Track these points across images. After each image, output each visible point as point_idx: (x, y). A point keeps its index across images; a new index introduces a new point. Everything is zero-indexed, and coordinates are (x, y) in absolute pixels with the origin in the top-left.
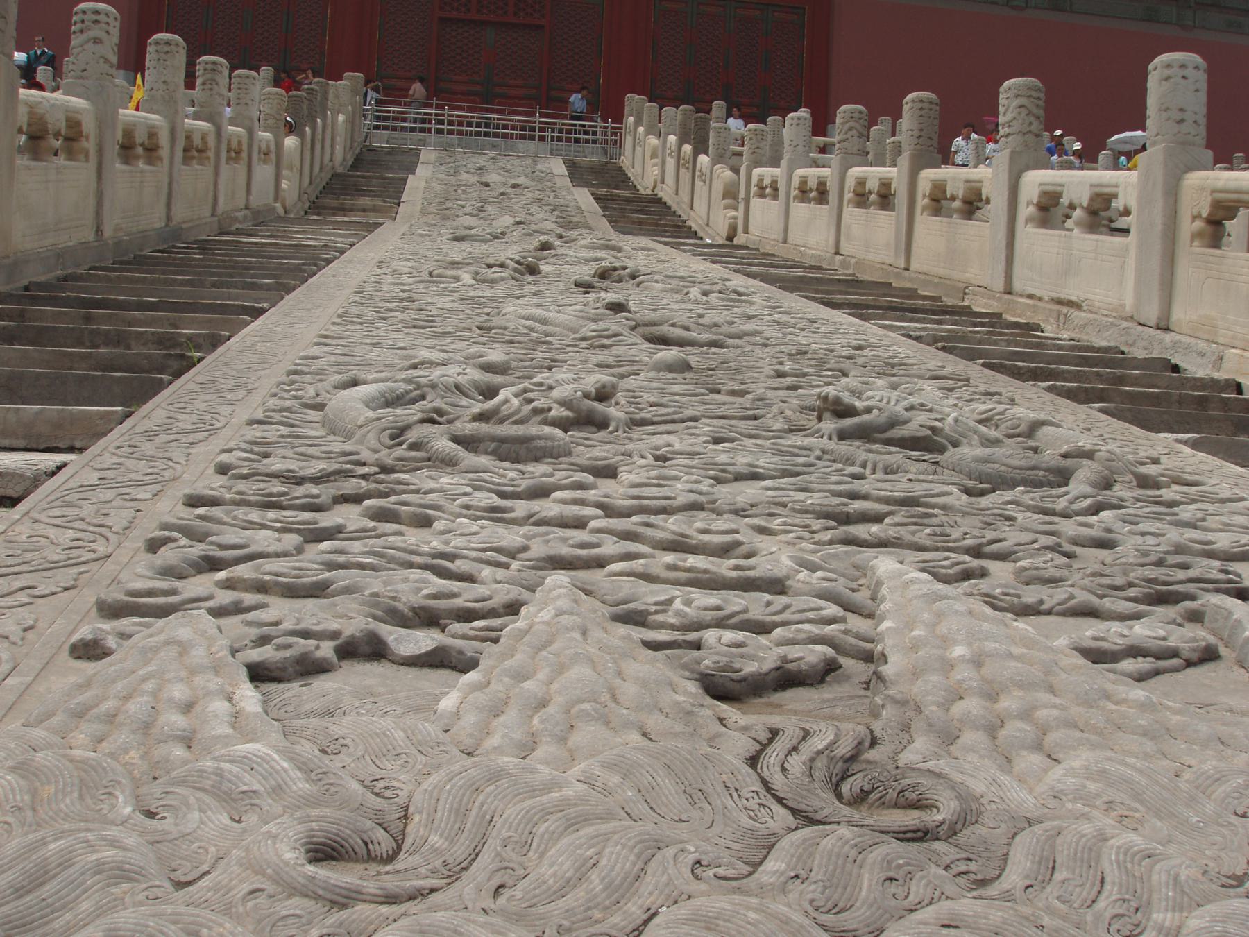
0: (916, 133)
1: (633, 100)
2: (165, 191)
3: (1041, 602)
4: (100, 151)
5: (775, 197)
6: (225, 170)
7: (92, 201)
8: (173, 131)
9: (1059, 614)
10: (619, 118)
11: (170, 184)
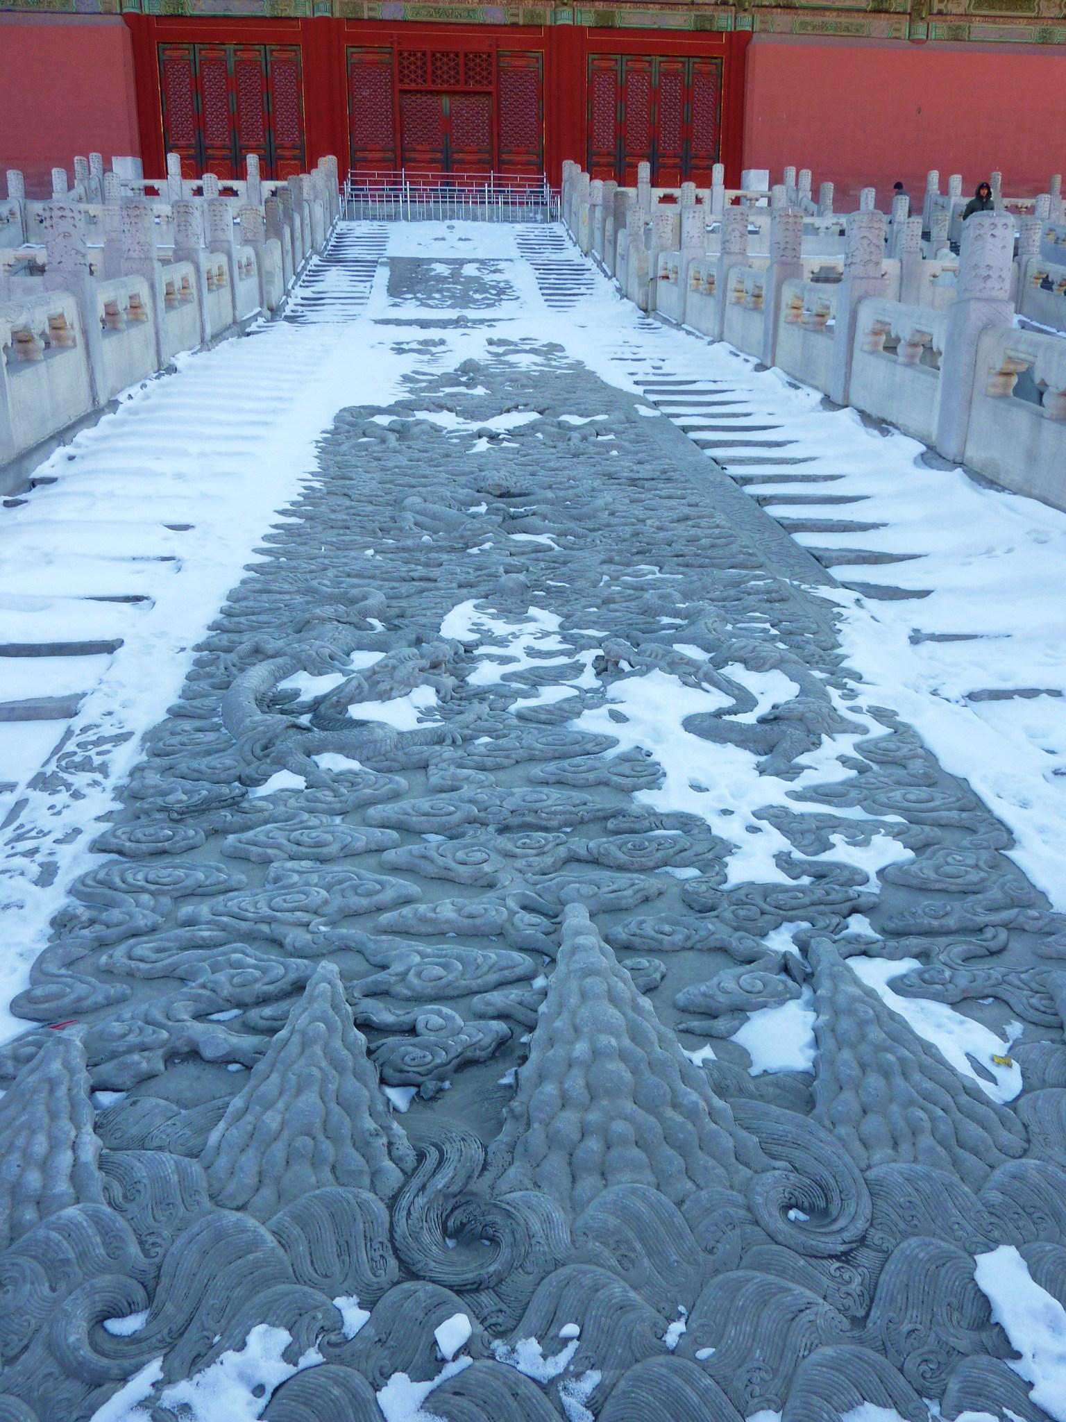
0: (782, 246)
1: (570, 168)
2: (154, 342)
3: (688, 938)
4: (85, 333)
5: (676, 283)
6: (209, 299)
7: (84, 378)
8: (152, 287)
9: (699, 950)
10: (556, 181)
11: (157, 333)
